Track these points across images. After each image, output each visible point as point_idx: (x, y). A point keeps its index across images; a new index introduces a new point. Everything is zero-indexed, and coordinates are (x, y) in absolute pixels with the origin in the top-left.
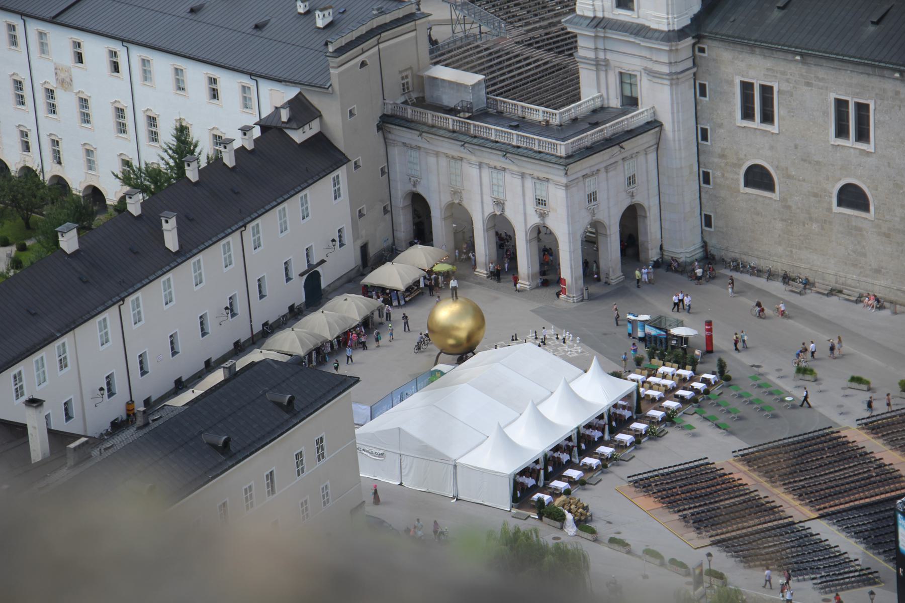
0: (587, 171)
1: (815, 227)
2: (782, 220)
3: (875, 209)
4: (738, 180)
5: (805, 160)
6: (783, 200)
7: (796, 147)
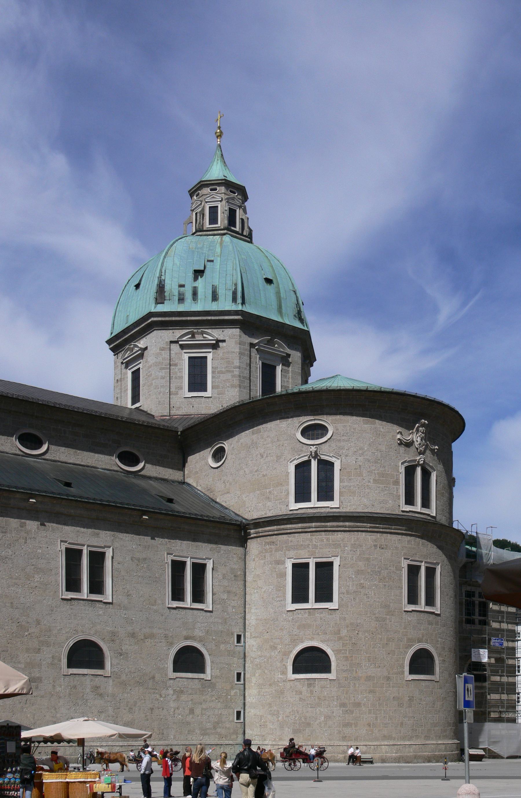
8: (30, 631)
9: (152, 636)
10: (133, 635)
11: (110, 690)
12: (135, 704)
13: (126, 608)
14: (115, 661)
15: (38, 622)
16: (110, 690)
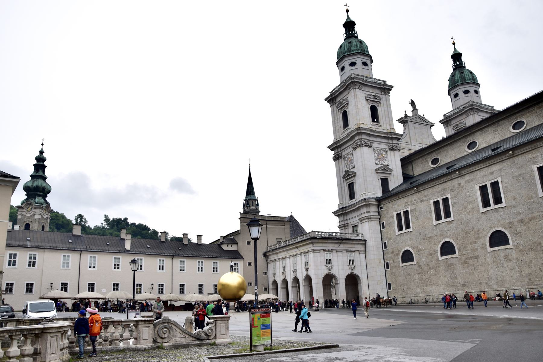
0: (327, 249)
1: (432, 272)
2: (418, 274)
3: (458, 250)
4: (399, 261)
5: (424, 239)
6: (418, 263)
7: (420, 234)
8: (471, 233)
9: (533, 218)
10: (522, 221)
11: (514, 256)
12: (531, 262)
13: (514, 207)
14: (514, 239)
15: (473, 228)
16: (514, 256)
